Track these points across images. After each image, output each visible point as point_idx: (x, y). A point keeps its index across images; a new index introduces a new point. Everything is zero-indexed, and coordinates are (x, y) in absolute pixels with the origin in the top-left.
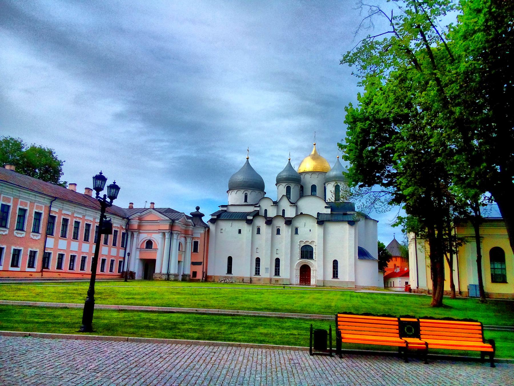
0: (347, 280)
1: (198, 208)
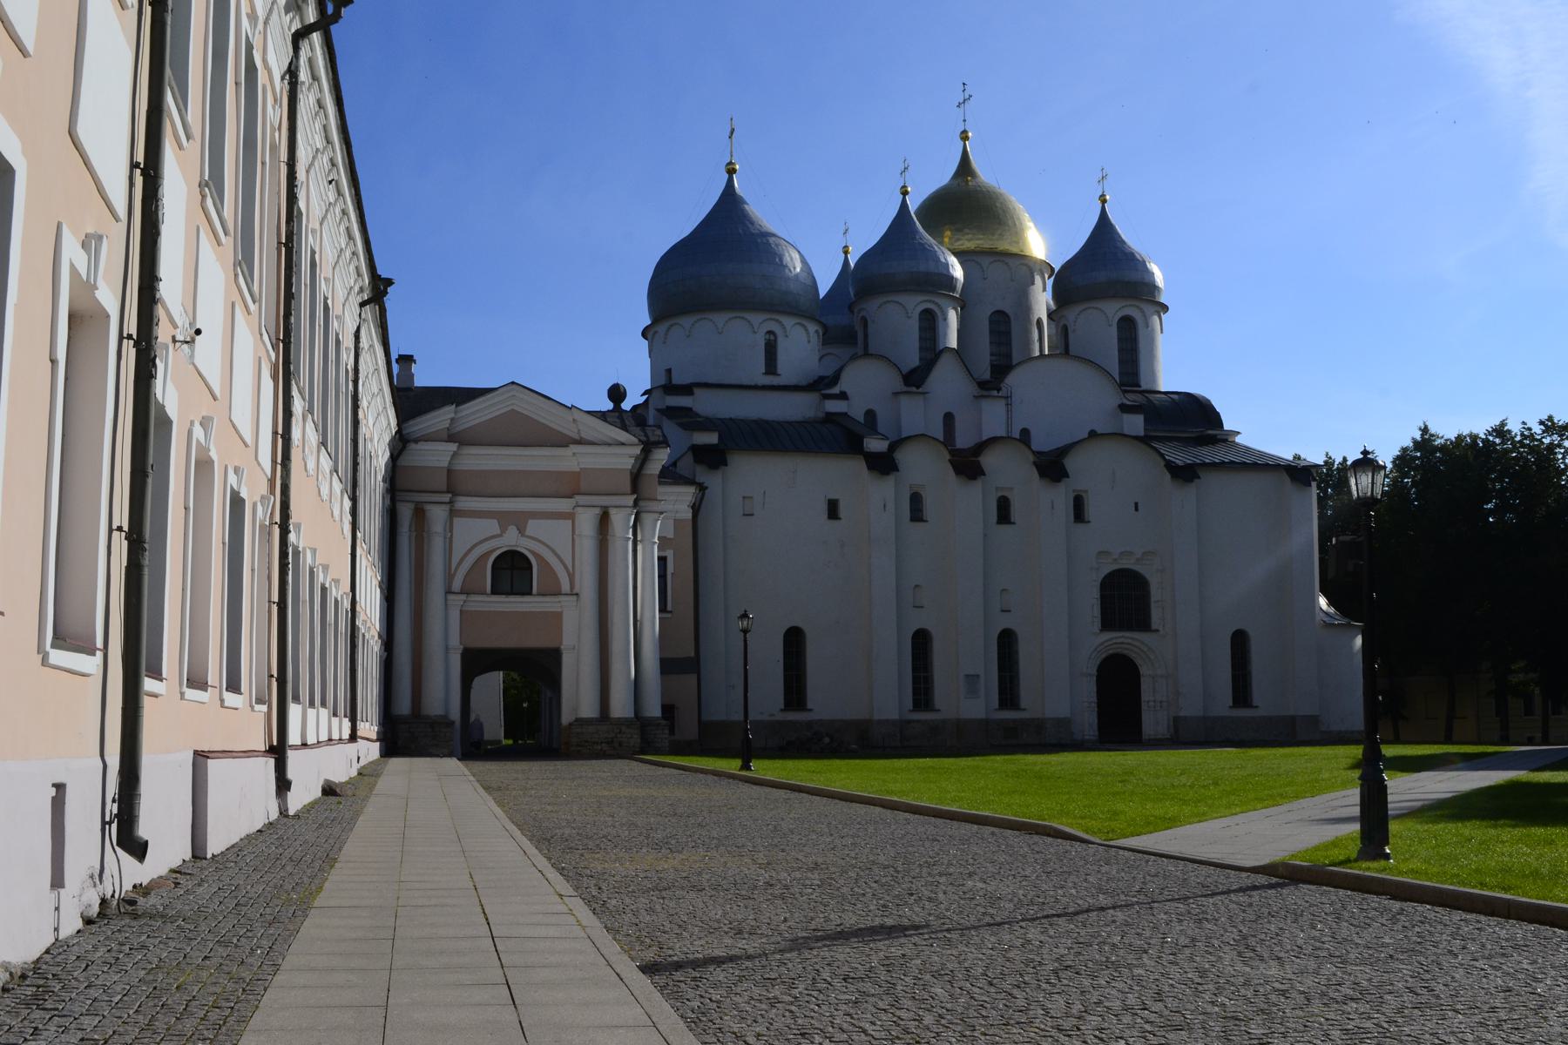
1: (616, 393)
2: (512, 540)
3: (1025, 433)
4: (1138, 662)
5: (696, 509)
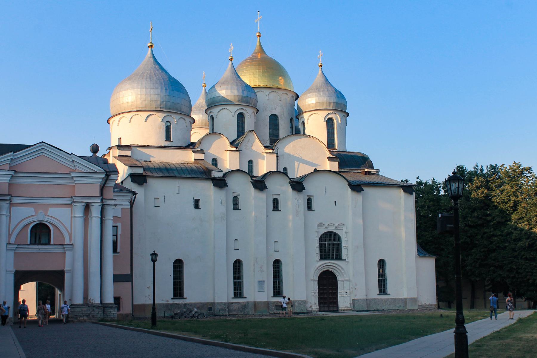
0: (405, 297)
2: (40, 217)
4: (337, 274)
5: (132, 204)
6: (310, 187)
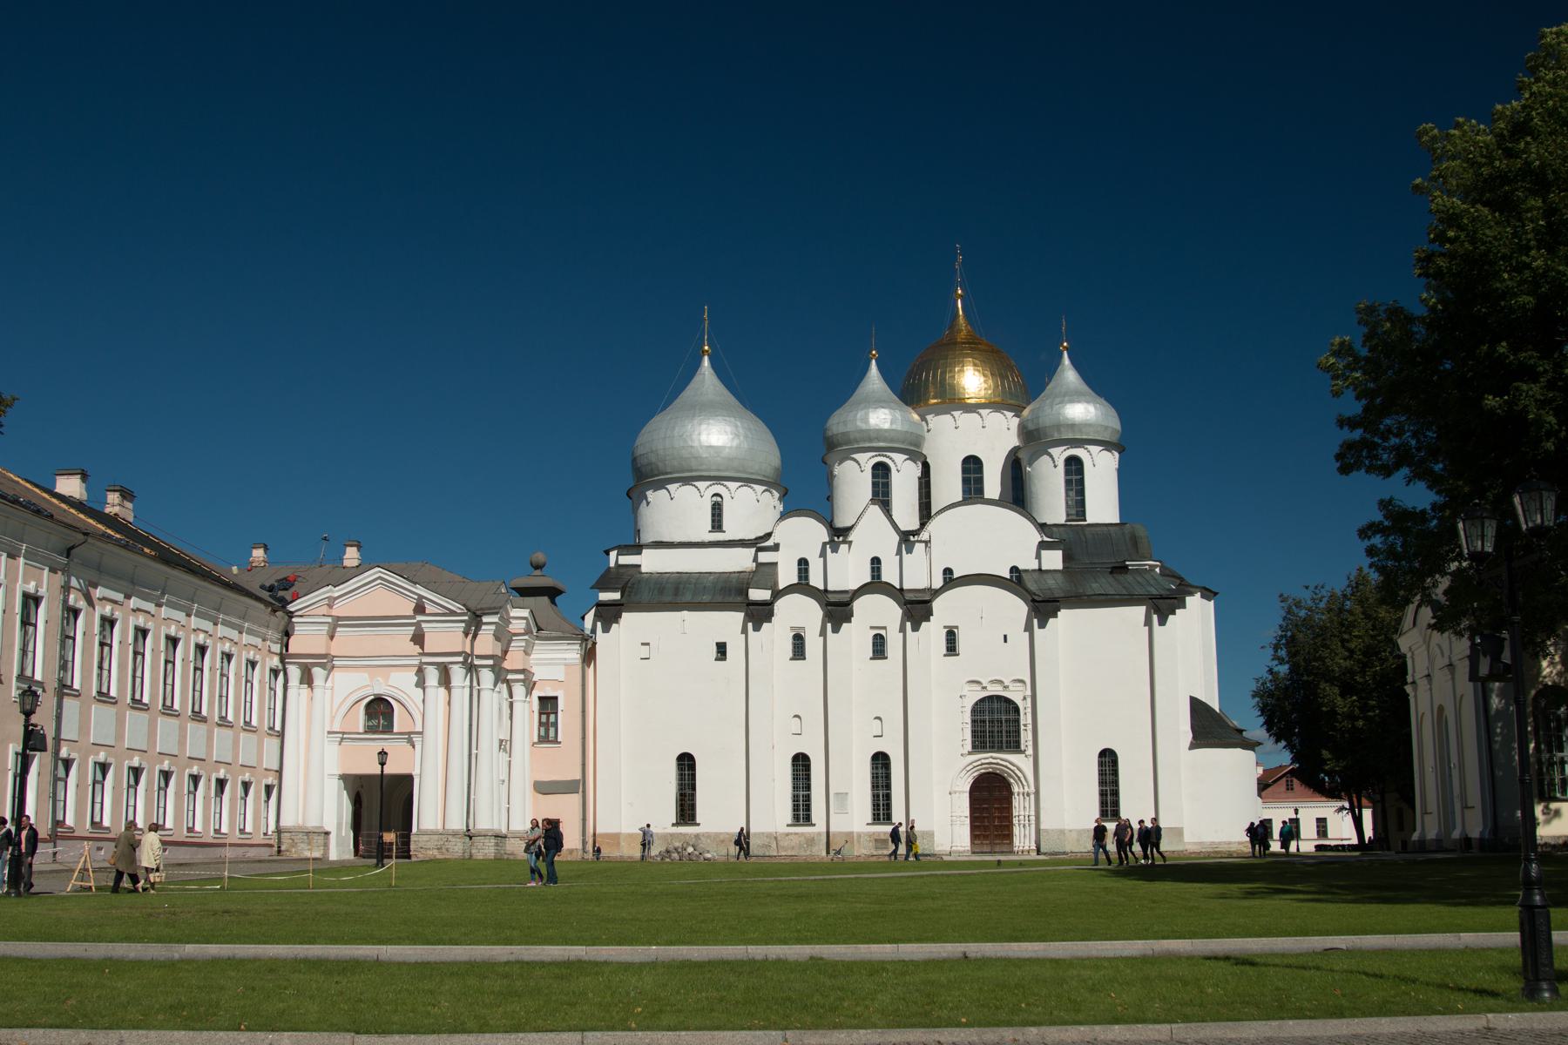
3: (948, 572)
6: (945, 609)
